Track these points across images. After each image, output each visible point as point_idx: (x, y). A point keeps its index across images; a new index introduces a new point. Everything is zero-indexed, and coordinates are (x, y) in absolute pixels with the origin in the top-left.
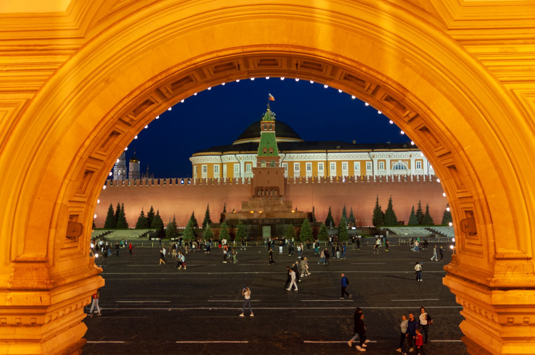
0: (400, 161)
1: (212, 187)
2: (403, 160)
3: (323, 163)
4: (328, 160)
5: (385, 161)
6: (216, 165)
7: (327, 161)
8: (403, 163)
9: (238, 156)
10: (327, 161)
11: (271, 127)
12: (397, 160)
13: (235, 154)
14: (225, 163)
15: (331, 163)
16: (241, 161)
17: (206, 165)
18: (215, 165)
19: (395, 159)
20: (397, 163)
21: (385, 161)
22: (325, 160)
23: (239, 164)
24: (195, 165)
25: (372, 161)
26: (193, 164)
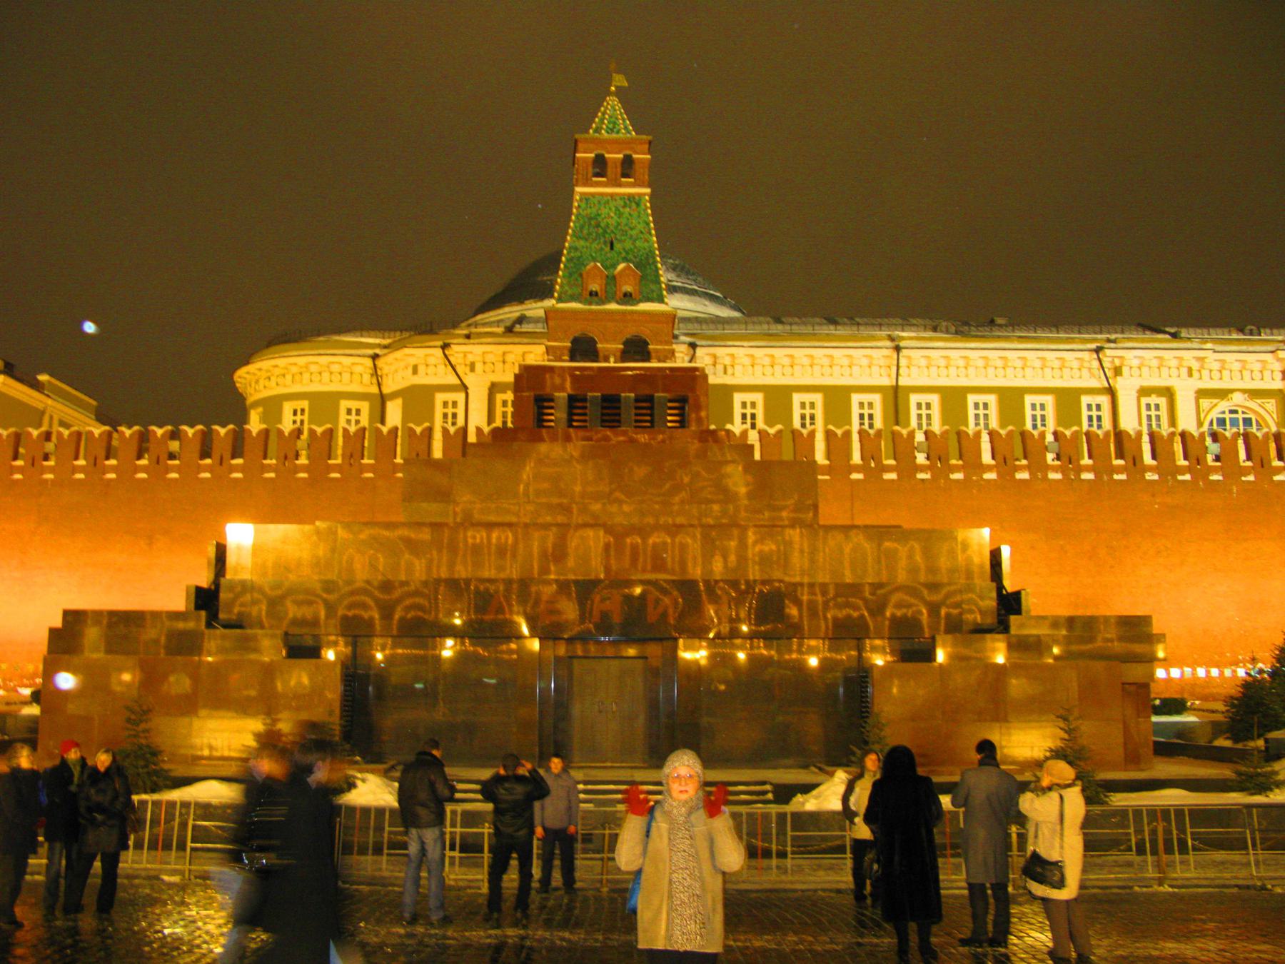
0: (1238, 398)
1: (301, 473)
2: (1254, 394)
3: (876, 398)
4: (903, 382)
5: (1168, 393)
6: (354, 405)
7: (896, 389)
8: (1252, 404)
9: (458, 351)
10: (896, 389)
11: (628, 166)
12: (1222, 394)
13: (445, 346)
14: (394, 395)
15: (914, 399)
16: (469, 380)
17: (305, 404)
18: (344, 404)
19: (1215, 385)
20: (1224, 405)
21: (1168, 393)
22: (887, 381)
23: (460, 397)
24: (256, 404)
25: (1111, 392)
26: (250, 400)
